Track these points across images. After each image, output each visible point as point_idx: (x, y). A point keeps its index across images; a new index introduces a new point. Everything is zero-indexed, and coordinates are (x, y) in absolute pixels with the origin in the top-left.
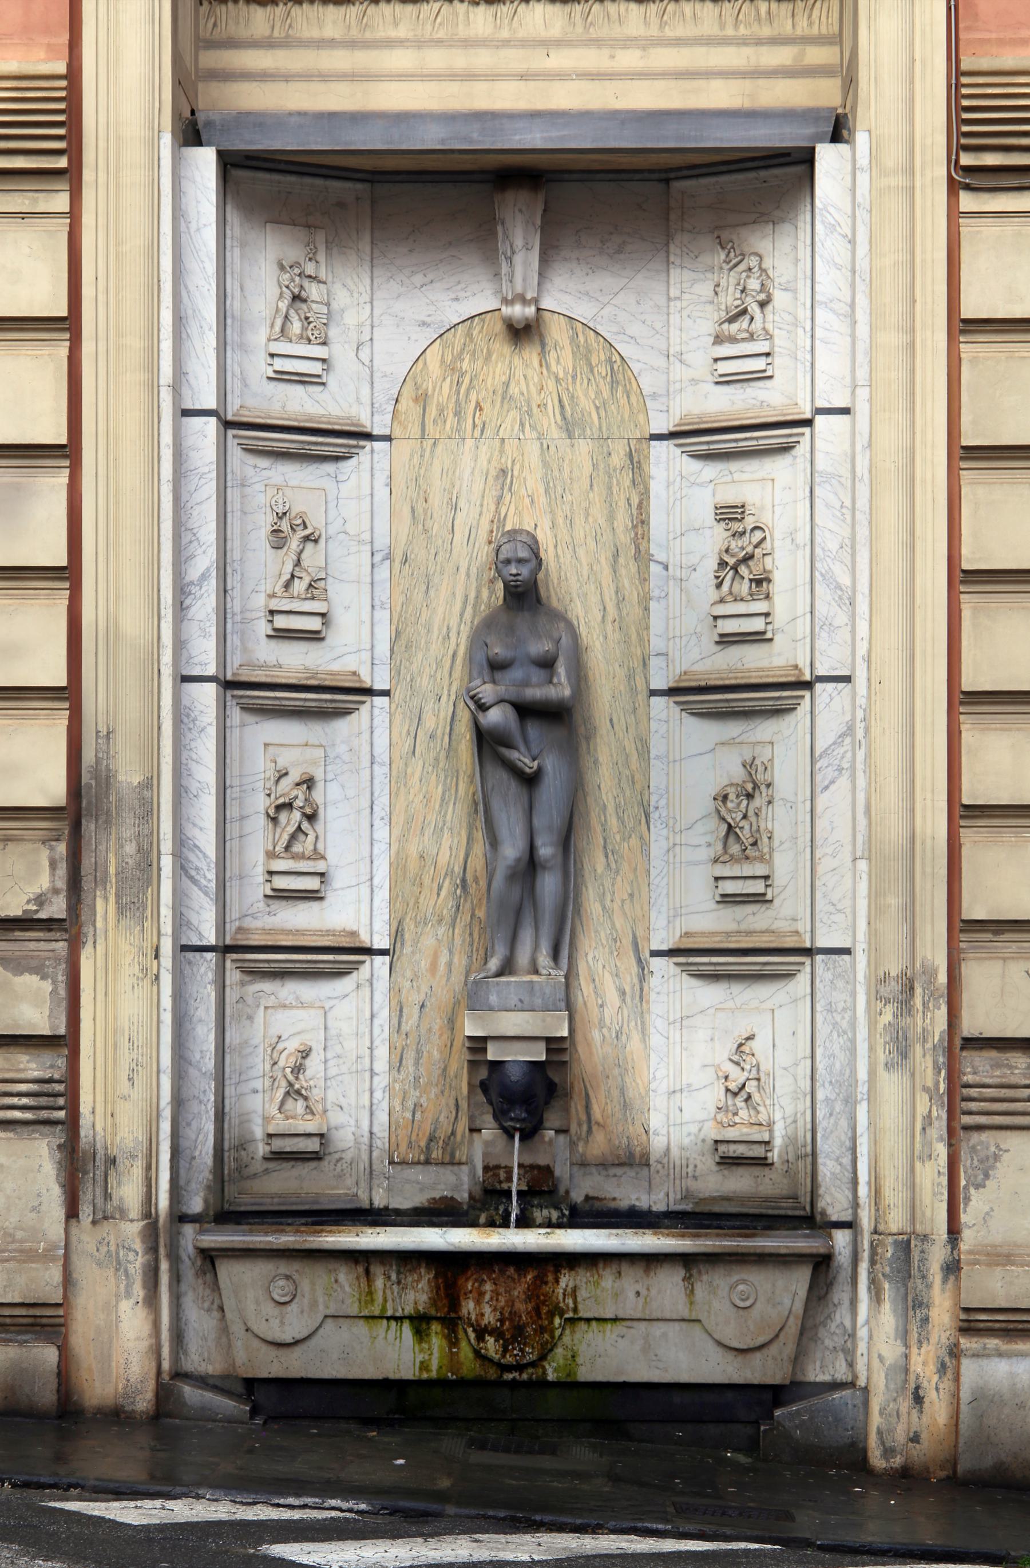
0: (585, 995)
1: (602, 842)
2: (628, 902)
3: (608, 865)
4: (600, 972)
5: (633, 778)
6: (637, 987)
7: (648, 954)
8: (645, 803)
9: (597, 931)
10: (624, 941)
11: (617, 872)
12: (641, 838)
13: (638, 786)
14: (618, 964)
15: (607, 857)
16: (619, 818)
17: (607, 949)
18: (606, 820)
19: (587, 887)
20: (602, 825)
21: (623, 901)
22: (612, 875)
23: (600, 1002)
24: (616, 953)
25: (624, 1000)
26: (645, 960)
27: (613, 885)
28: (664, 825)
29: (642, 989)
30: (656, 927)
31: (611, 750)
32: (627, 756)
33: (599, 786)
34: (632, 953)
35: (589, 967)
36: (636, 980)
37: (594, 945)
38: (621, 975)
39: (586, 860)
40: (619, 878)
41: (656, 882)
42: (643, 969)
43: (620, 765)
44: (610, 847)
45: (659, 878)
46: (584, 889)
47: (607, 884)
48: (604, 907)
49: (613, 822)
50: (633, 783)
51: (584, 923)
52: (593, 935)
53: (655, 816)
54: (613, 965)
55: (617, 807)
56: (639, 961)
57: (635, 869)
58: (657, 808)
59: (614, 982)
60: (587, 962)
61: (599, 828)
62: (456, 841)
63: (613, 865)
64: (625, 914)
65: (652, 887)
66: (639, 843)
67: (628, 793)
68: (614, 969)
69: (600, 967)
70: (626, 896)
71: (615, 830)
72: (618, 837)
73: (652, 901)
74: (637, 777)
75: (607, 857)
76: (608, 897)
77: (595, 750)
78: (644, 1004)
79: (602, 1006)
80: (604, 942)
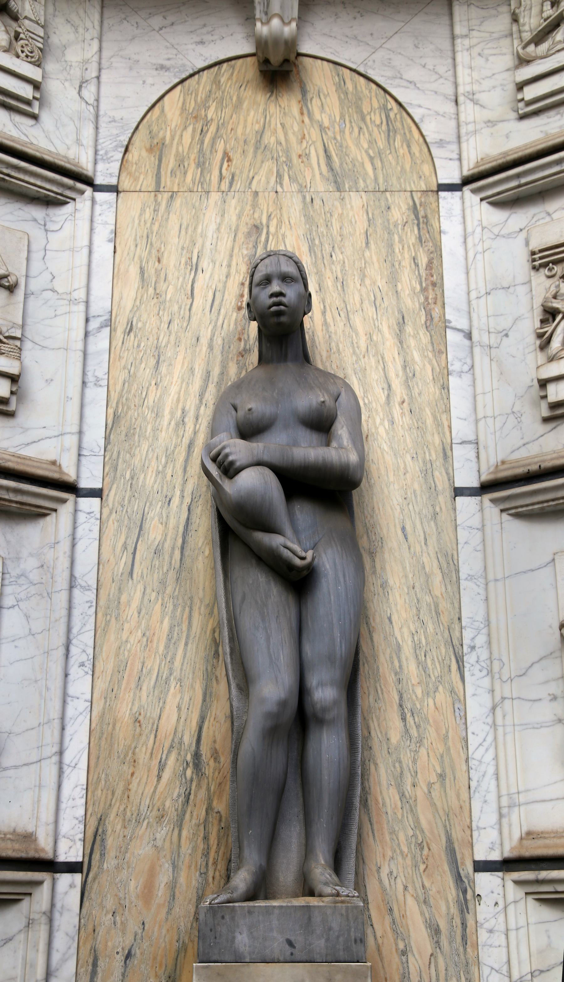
0: (379, 934)
1: (397, 698)
2: (437, 786)
3: (407, 731)
4: (401, 897)
5: (437, 606)
6: (457, 921)
7: (470, 868)
8: (456, 642)
9: (393, 832)
10: (433, 846)
11: (420, 741)
12: (452, 691)
13: (444, 619)
14: (427, 884)
15: (404, 719)
16: (419, 663)
17: (409, 861)
18: (400, 667)
19: (376, 764)
20: (396, 674)
21: (430, 785)
22: (413, 747)
23: (401, 946)
24: (422, 867)
25: (438, 942)
26: (467, 877)
27: (415, 761)
28: (485, 672)
29: (464, 925)
30: (481, 825)
31: (404, 568)
32: (428, 577)
33: (390, 619)
34: (446, 867)
35: (384, 890)
36: (454, 910)
37: (389, 853)
38: (432, 901)
39: (374, 725)
40: (423, 751)
41: (478, 755)
42: (465, 892)
43: (417, 589)
44: (408, 705)
45: (482, 750)
46: (372, 767)
47: (406, 758)
48: (402, 795)
49: (411, 669)
50: (438, 614)
51: (374, 820)
52: (387, 837)
53: (470, 659)
54: (418, 885)
55: (417, 647)
56: (458, 879)
57: (446, 737)
58: (473, 648)
59: (422, 914)
60: (380, 881)
61: (391, 678)
62: (187, 698)
63: (414, 732)
64: (433, 805)
65: (471, 763)
66: (449, 700)
67: (430, 627)
68: (420, 891)
69: (400, 888)
70: (433, 778)
71: (415, 680)
72: (419, 691)
73: (473, 784)
74: (444, 605)
75: (404, 719)
76: (408, 780)
77: (383, 569)
78: (469, 950)
79: (404, 953)
80: (405, 849)
